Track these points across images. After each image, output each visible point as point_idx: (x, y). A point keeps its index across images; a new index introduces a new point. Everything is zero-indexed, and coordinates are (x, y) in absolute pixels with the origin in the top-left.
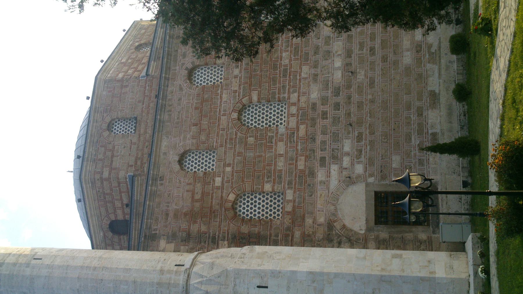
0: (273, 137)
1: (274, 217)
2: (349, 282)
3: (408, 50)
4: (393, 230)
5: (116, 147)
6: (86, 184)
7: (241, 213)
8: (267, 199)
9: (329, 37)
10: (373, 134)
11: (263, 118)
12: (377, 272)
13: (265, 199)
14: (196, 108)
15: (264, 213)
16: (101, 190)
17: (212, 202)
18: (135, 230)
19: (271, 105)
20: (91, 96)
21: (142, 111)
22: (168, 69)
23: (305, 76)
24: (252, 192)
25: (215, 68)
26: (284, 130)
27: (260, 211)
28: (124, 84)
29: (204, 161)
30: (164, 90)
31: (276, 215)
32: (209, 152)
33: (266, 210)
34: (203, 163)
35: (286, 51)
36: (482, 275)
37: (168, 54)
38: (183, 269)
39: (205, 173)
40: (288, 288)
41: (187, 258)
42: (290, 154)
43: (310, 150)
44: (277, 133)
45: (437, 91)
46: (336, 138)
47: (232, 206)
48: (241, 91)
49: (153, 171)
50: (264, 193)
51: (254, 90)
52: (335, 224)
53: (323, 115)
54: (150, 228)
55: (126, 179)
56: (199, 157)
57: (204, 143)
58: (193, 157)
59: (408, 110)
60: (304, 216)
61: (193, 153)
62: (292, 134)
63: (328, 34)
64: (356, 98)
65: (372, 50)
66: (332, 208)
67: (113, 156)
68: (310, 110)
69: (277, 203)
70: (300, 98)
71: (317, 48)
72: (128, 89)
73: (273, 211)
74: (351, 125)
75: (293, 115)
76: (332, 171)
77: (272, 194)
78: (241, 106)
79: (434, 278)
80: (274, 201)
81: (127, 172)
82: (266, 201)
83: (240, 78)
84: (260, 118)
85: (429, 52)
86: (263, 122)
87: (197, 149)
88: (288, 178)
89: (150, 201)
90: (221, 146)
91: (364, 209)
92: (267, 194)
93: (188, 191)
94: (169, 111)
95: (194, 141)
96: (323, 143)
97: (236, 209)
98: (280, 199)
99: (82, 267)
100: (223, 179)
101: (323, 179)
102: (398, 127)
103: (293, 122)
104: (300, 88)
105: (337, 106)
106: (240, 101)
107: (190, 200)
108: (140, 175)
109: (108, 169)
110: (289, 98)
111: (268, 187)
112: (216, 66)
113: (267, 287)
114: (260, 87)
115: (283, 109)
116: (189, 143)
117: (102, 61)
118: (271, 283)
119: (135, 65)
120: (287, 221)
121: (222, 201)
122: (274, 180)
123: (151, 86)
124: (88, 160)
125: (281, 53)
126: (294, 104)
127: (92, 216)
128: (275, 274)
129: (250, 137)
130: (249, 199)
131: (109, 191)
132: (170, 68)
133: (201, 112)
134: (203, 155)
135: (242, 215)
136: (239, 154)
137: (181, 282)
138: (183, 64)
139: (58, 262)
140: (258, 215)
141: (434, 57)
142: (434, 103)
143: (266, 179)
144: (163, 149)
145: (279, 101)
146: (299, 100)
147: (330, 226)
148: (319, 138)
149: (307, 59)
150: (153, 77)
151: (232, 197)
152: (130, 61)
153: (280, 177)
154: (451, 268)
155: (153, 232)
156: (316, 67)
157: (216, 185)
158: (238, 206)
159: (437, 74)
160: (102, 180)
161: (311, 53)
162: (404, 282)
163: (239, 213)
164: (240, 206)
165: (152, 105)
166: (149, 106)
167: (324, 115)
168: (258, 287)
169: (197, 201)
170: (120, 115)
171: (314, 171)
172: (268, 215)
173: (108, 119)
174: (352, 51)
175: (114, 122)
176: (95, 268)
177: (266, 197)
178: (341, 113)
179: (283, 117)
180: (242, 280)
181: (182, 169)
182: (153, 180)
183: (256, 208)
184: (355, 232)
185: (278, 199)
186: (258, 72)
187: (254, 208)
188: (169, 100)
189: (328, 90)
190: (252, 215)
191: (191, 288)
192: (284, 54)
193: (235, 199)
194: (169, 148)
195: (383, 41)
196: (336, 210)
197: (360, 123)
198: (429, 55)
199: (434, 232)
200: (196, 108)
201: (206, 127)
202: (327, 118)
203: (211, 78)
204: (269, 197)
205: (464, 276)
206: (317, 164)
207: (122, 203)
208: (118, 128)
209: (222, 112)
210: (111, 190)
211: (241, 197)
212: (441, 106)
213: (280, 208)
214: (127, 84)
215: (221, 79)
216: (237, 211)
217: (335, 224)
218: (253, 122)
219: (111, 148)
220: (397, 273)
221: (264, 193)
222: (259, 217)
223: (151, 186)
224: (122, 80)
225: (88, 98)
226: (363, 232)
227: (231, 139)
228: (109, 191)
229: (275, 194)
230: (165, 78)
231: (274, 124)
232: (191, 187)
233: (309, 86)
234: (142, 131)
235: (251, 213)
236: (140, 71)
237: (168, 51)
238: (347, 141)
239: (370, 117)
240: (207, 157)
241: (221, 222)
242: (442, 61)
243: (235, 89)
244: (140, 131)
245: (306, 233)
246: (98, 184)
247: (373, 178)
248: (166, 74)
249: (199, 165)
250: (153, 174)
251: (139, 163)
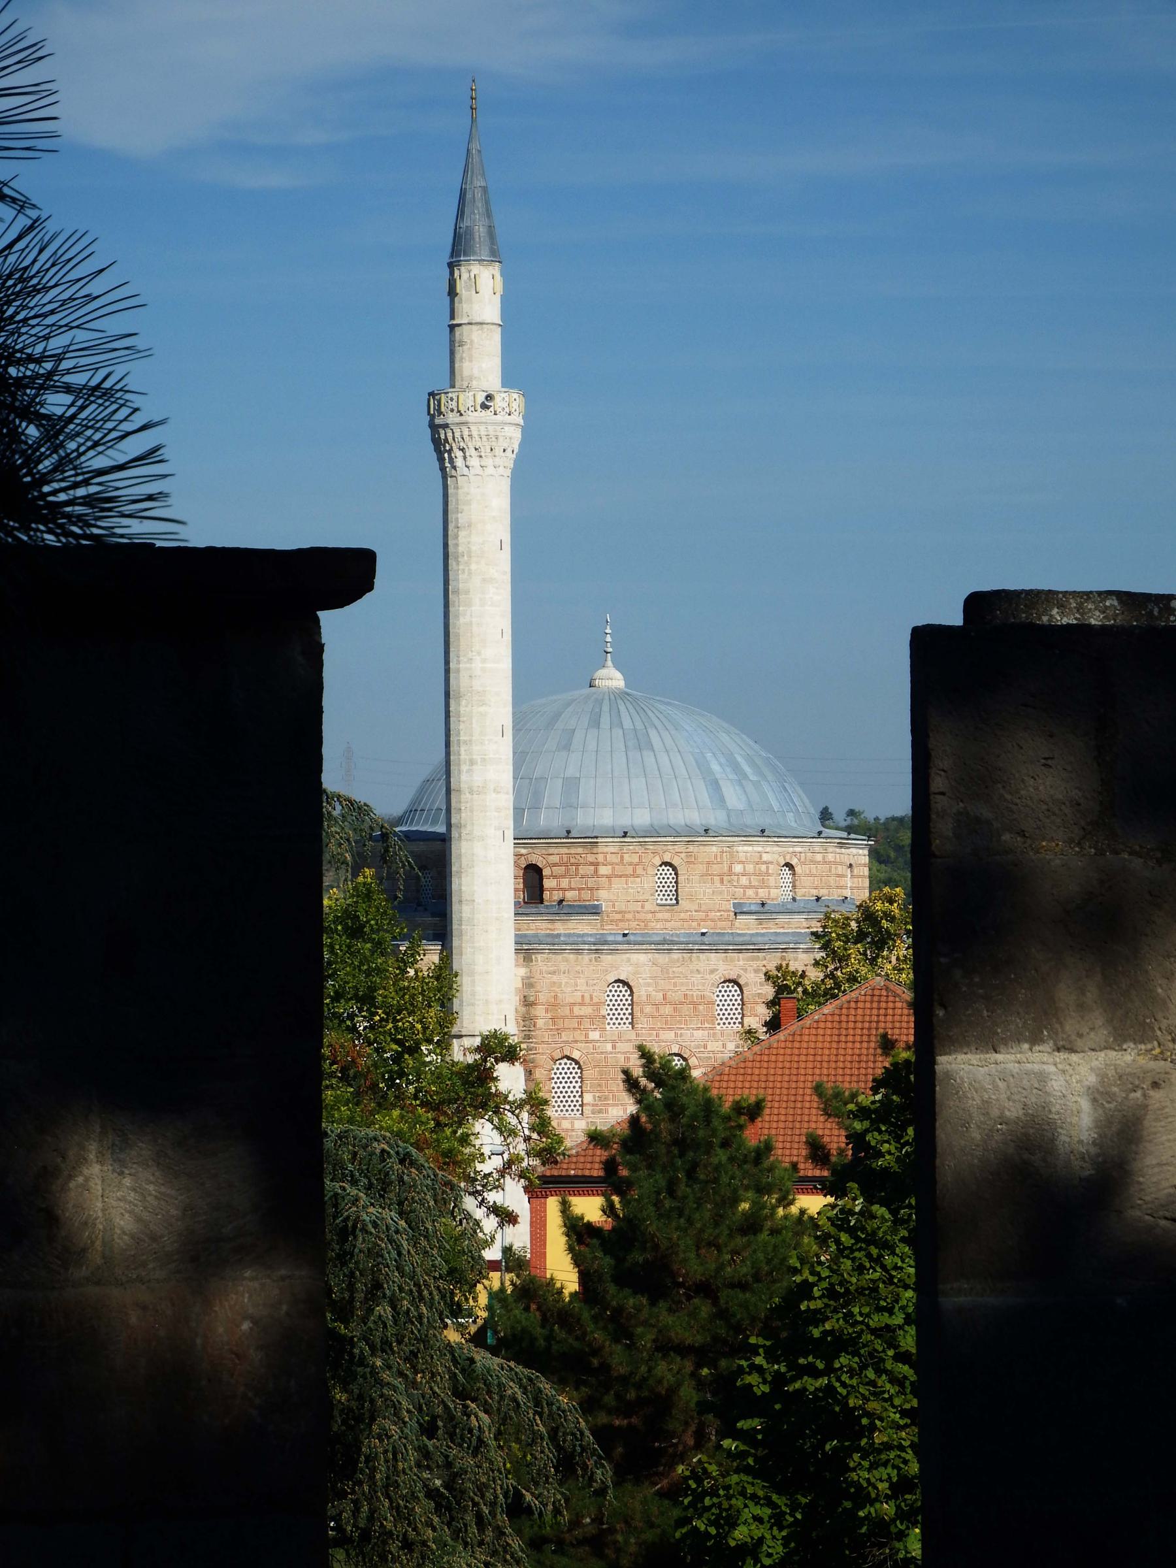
16: (582, 861)
72: (719, 885)
83: (722, 1052)
95: (644, 998)
109: (610, 872)
116: (641, 993)
122: (597, 1105)
131: (581, 872)
133: (681, 1003)
144: (635, 957)
153: (600, 1112)
160: (596, 864)
166: (693, 920)
201: (662, 1012)
207: (564, 890)
219: (638, 872)
232: (587, 1000)
234: (659, 916)
244: (660, 911)
251: (619, 916)
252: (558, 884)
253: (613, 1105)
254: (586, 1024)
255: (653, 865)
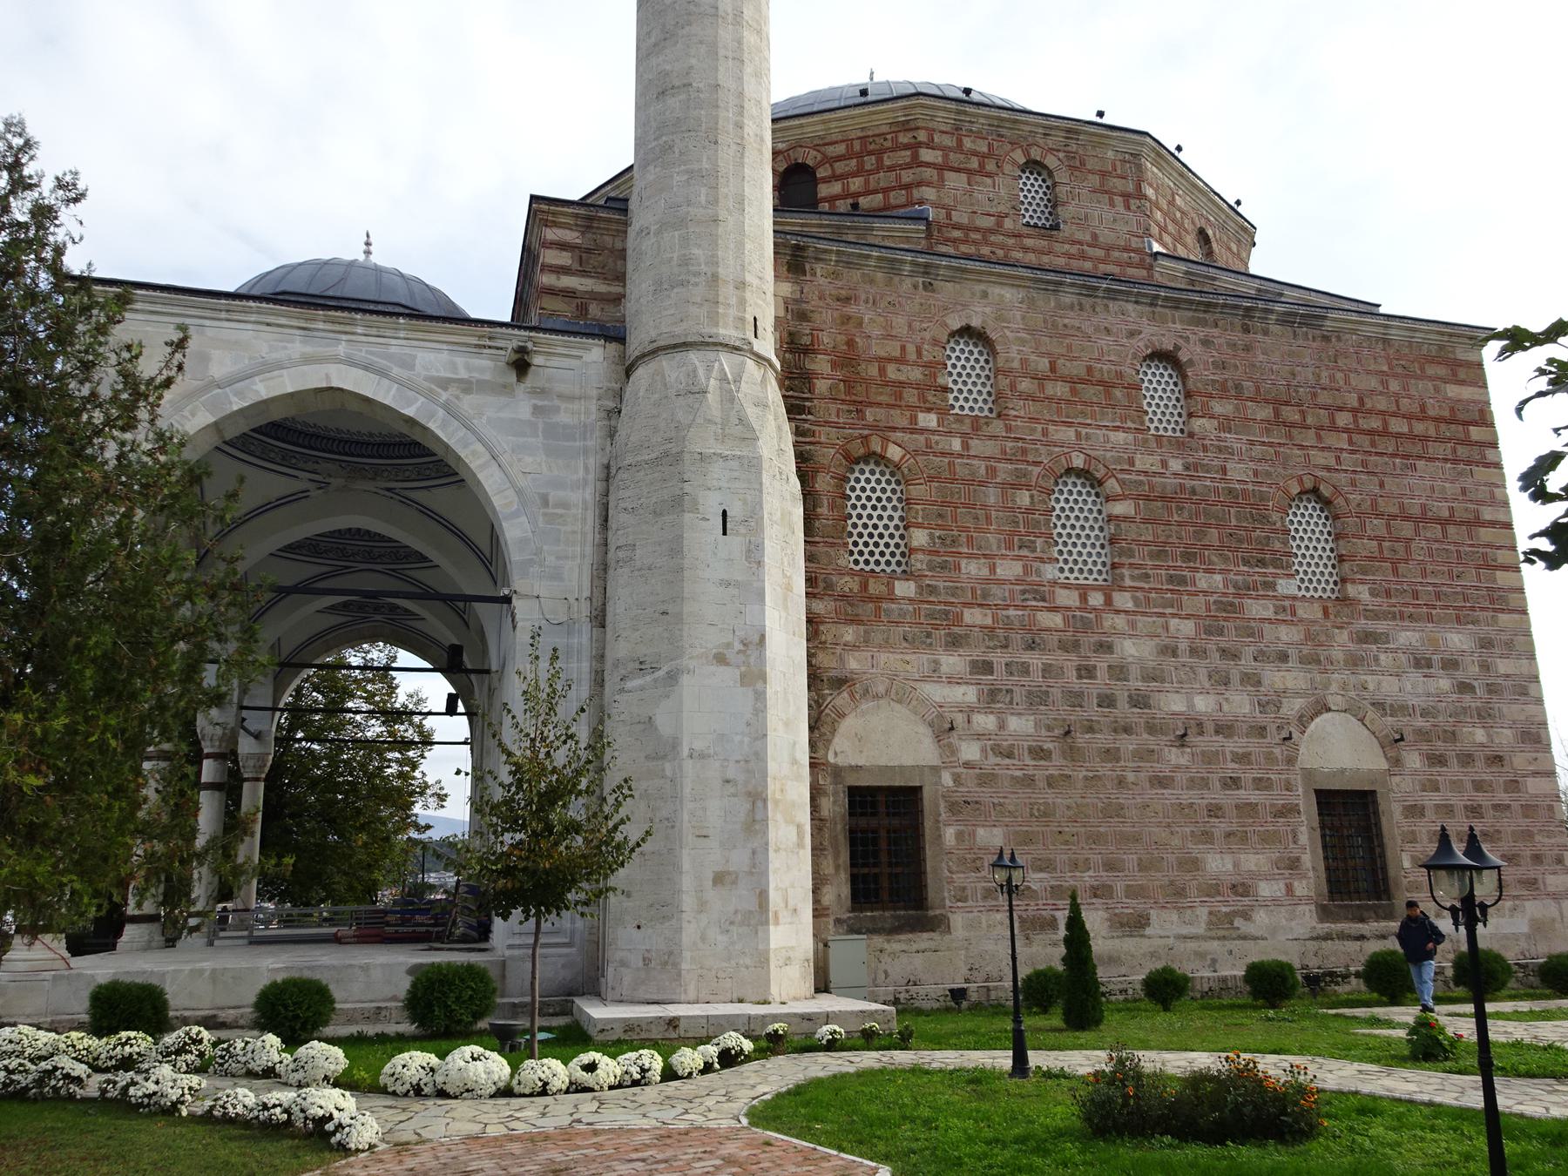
0: (1034, 551)
1: (852, 553)
2: (748, 724)
3: (1236, 865)
4: (839, 827)
5: (989, 181)
6: (905, 108)
7: (857, 474)
8: (892, 536)
9: (1259, 683)
10: (1049, 785)
11: (1073, 527)
12: (772, 788)
13: (892, 530)
14: (1089, 369)
15: (860, 529)
16: (888, 144)
17: (879, 404)
18: (802, 225)
19: (1102, 546)
20: (1104, 121)
21: (1074, 242)
22: (1176, 304)
23: (1172, 628)
24: (907, 502)
25: (1180, 415)
26: (1050, 577)
27: (865, 520)
28: (1132, 201)
29: (970, 386)
30: (1129, 293)
31: (856, 556)
32: (990, 399)
33: (866, 532)
34: (965, 383)
35: (1225, 581)
36: (824, 1031)
37: (1209, 305)
38: (750, 335)
39: (946, 389)
40: (727, 584)
41: (767, 345)
42: (994, 589)
43: (1006, 638)
44: (1042, 560)
45: (1148, 931)
46: (1037, 699)
47: (875, 453)
48: (1134, 477)
49: (947, 267)
50: (906, 528)
51: (1137, 506)
52: (845, 694)
53: (1087, 668)
54: (818, 259)
55: (921, 203)
56: (978, 376)
57: (1013, 387)
58: (977, 360)
59: (1104, 865)
60: (859, 622)
61: (987, 361)
62: (1041, 594)
63: (1266, 682)
64: (1128, 744)
65: (1233, 783)
66: (881, 689)
67: (969, 172)
68: (1096, 638)
69: (883, 560)
70: (1123, 615)
71: (1235, 656)
72: (1122, 210)
73: (866, 551)
74: (1068, 733)
75: (1084, 598)
76: (963, 689)
77: (902, 549)
78: (1098, 475)
79: (767, 923)
80: (887, 552)
81: (936, 206)
82: (886, 533)
84: (1073, 521)
85: (1235, 914)
86: (1064, 526)
87: (997, 371)
88: (941, 584)
89: (879, 258)
90: (1009, 429)
91: (883, 762)
92: (902, 537)
93: (903, 348)
94: (1080, 304)
95: (1016, 364)
96: (1025, 669)
97: (867, 463)
98: (894, 566)
99: (741, 94)
100: (934, 432)
101: (944, 669)
102: (1066, 843)
103: (1068, 598)
104: (1144, 614)
105: (1107, 701)
106: (1111, 474)
107: (883, 354)
108: (929, 236)
110: (1122, 589)
111: (919, 537)
112: (1184, 418)
113: (725, 533)
114: (1145, 521)
115: (1095, 575)
116: (1012, 353)
117: (1179, 148)
118: (735, 542)
119: (1171, 227)
120: (849, 584)
121: (885, 431)
123: (1130, 265)
124: (959, 112)
125: (1222, 572)
126: (1108, 601)
127: (824, 122)
128: (754, 555)
129: (1032, 497)
130: (889, 494)
131: (887, 162)
132: (1177, 308)
133: (1083, 381)
134: (984, 384)
135: (852, 477)
136: (992, 471)
137: (722, 331)
138: (1187, 339)
139: (749, 38)
140: (854, 513)
141: (1222, 925)
142: (1122, 925)
143: (937, 533)
144: (996, 291)
145: (1114, 566)
146: (1118, 612)
147: (840, 683)
148: (1035, 660)
149: (1208, 631)
150: (1151, 268)
151: (894, 453)
152: (1178, 215)
154: (788, 961)
155: (807, 267)
156: (1193, 651)
157: (921, 416)
158: (872, 466)
159: (1185, 931)
161: (1223, 642)
162: (754, 853)
163: (857, 468)
164: (872, 472)
165: (1088, 265)
167: (1087, 672)
168: (724, 513)
169: (882, 371)
170: (1062, 191)
171: (961, 646)
172: (855, 538)
173: (1051, 161)
174: (1230, 736)
175: (1045, 175)
176: (740, 126)
177: (897, 534)
178: (1093, 711)
179: (1076, 574)
180: (736, 474)
181: (952, 334)
182: (927, 266)
183: (869, 510)
184: (829, 741)
185: (893, 561)
186: (1176, 518)
187: (869, 505)
188: (1107, 306)
189: (1144, 679)
190: (853, 501)
191: (711, 355)
192: (1218, 577)
193: (889, 460)
194: (997, 303)
195: (1252, 807)
196: (877, 697)
197: (1072, 753)
198: (1227, 914)
199: (838, 921)
200: (1089, 369)
202: (1080, 677)
203: (1158, 406)
204: (897, 540)
205: (774, 990)
206: (977, 654)
207: (859, 194)
208: (1031, 189)
209: (1084, 431)
210: (891, 169)
211: (892, 474)
212: (1117, 941)
213: (872, 566)
214: (1133, 208)
215: (1157, 429)
216: (862, 466)
217: (845, 694)
218: (1062, 504)
220: (772, 835)
221: (906, 528)
222: (850, 516)
223: (914, 263)
224: (1142, 196)
225: (1100, 114)
226: (831, 759)
227: (1024, 451)
228: (887, 162)
229: (903, 554)
230: (1157, 297)
231: (1061, 553)
232: (912, 356)
233: (1152, 636)
234: (1029, 242)
235: (859, 498)
236: (1160, 241)
237: (1216, 305)
238: (1032, 723)
239: (1086, 778)
240: (980, 392)
241: (836, 426)
242: (1216, 943)
243: (1137, 463)
244: (1029, 236)
245: (821, 628)
246: (904, 139)
247: (951, 783)
248: (1166, 299)
249: (960, 375)
250: (938, 267)
251: (957, 234)
252: (845, 188)
253: (970, 556)
254: (911, 396)
255: (1014, 162)
